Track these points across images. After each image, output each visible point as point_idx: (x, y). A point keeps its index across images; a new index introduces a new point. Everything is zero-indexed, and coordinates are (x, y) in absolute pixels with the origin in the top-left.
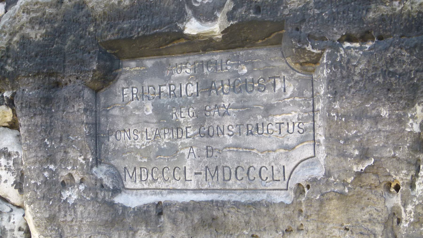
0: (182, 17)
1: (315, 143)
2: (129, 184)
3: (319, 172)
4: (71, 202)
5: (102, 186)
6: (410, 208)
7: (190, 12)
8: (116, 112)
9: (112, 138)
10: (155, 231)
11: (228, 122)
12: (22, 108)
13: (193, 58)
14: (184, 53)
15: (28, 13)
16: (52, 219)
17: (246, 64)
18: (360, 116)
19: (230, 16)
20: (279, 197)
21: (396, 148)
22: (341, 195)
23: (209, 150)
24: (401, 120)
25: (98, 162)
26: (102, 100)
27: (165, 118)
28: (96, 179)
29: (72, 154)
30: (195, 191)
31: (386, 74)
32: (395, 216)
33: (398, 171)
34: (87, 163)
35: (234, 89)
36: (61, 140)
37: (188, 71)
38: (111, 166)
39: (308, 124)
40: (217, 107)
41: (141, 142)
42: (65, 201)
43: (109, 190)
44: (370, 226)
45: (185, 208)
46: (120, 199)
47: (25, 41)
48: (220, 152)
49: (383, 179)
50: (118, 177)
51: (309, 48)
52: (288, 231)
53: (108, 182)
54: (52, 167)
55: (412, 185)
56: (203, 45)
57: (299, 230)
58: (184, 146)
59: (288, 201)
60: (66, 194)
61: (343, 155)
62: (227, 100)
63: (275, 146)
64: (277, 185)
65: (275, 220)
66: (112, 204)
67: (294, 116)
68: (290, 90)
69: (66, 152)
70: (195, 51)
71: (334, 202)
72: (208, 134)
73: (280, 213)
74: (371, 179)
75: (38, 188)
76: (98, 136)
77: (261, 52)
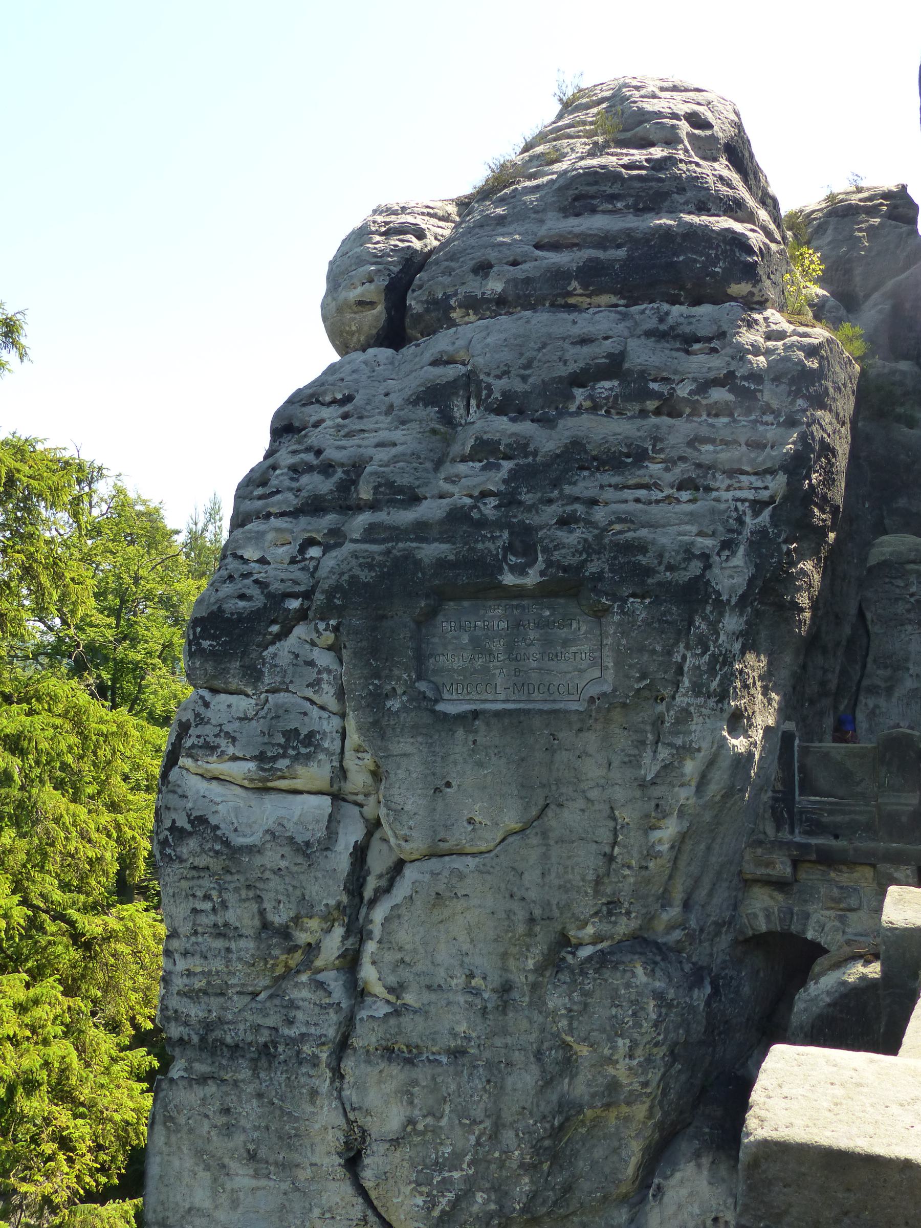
0: (501, 571)
1: (603, 668)
2: (446, 696)
3: (607, 688)
4: (394, 709)
5: (425, 697)
6: (672, 713)
7: (506, 567)
8: (436, 640)
9: (432, 660)
10: (471, 732)
11: (533, 650)
12: (348, 634)
13: (504, 602)
14: (496, 599)
15: (357, 557)
16: (376, 723)
17: (548, 608)
18: (641, 649)
19: (542, 574)
20: (574, 706)
21: (665, 673)
22: (624, 705)
23: (517, 671)
24: (669, 653)
25: (419, 678)
26: (424, 631)
27: (478, 646)
28: (420, 692)
29: (396, 672)
30: (504, 701)
31: (659, 621)
32: (660, 719)
33: (665, 688)
34: (411, 679)
35: (538, 626)
36: (387, 660)
37: (500, 611)
38: (430, 682)
39: (597, 654)
40: (524, 640)
41: (458, 664)
42: (389, 709)
43: (430, 700)
44: (642, 726)
45: (498, 714)
46: (440, 707)
47: (354, 580)
48: (526, 672)
49: (654, 694)
50: (438, 689)
51: (604, 600)
52: (580, 730)
53: (430, 694)
54: (376, 682)
55: (674, 698)
56: (518, 593)
57: (589, 729)
58: (496, 668)
59: (581, 709)
60: (389, 703)
61: (627, 677)
62: (532, 635)
63: (570, 669)
64: (571, 697)
65: (570, 723)
66: (433, 712)
67: (586, 647)
68: (584, 629)
69: (391, 670)
70: (506, 598)
71: (619, 709)
72: (516, 659)
73: (574, 718)
74: (646, 693)
75: (363, 698)
76: (420, 659)
77: (562, 601)
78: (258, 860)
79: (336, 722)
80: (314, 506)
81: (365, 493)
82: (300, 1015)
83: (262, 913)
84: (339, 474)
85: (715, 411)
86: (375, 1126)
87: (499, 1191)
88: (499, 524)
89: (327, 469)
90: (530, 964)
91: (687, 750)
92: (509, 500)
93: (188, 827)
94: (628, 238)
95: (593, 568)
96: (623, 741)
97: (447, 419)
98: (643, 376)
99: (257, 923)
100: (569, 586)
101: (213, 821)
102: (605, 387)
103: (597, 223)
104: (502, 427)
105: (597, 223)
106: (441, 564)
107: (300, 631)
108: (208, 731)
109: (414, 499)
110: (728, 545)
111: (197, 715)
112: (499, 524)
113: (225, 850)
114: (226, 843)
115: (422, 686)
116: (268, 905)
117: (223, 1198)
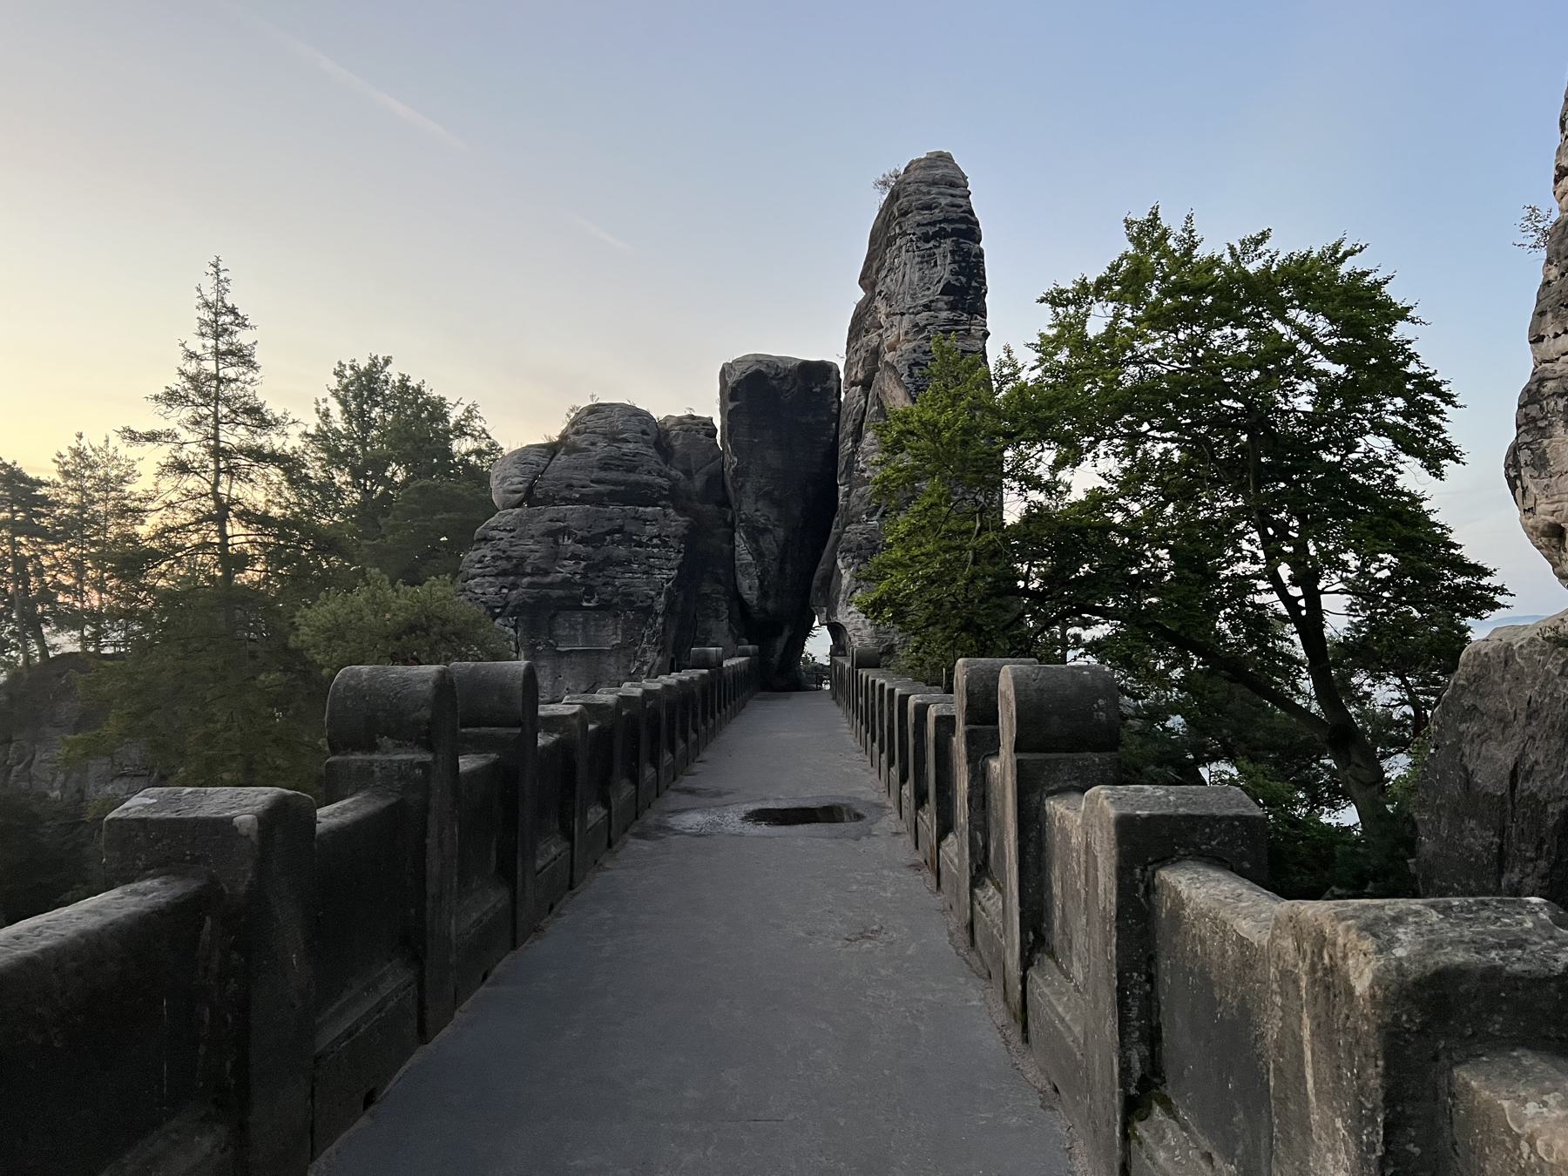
27: (572, 627)
76: (551, 631)
80: (504, 573)
81: (529, 570)
85: (655, 546)
88: (582, 585)
89: (509, 558)
91: (644, 663)
92: (584, 576)
94: (624, 483)
95: (616, 600)
96: (624, 661)
97: (556, 542)
98: (631, 534)
100: (605, 606)
103: (612, 475)
105: (612, 475)
106: (560, 598)
107: (499, 621)
109: (547, 573)
110: (659, 594)
112: (582, 585)
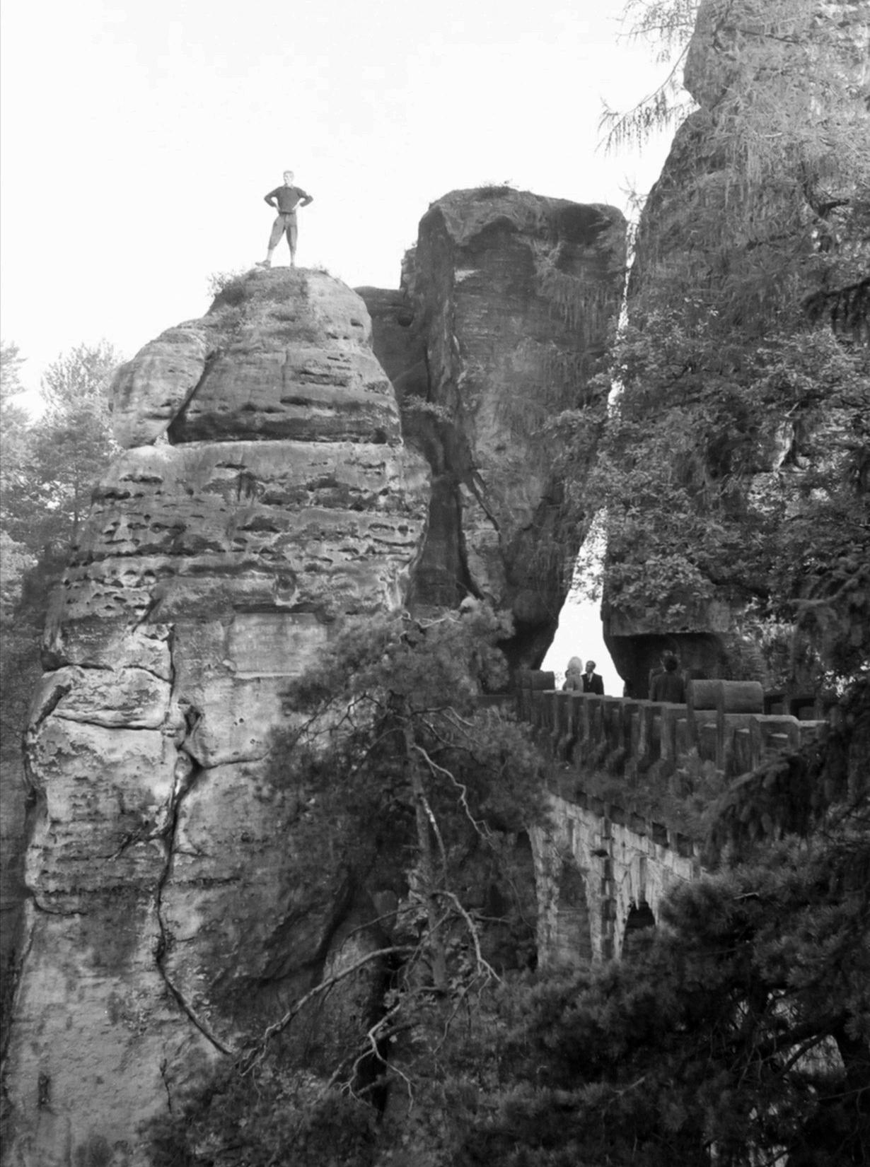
56: (283, 610)
78: (121, 771)
79: (168, 686)
82: (138, 868)
83: (121, 804)
84: (166, 533)
86: (180, 934)
87: (252, 962)
90: (279, 824)
93: (73, 753)
99: (117, 810)
101: (91, 746)
102: (326, 491)
104: (268, 512)
108: (87, 691)
111: (76, 682)
113: (100, 766)
114: (100, 760)
115: (226, 663)
116: (126, 799)
117: (74, 996)
